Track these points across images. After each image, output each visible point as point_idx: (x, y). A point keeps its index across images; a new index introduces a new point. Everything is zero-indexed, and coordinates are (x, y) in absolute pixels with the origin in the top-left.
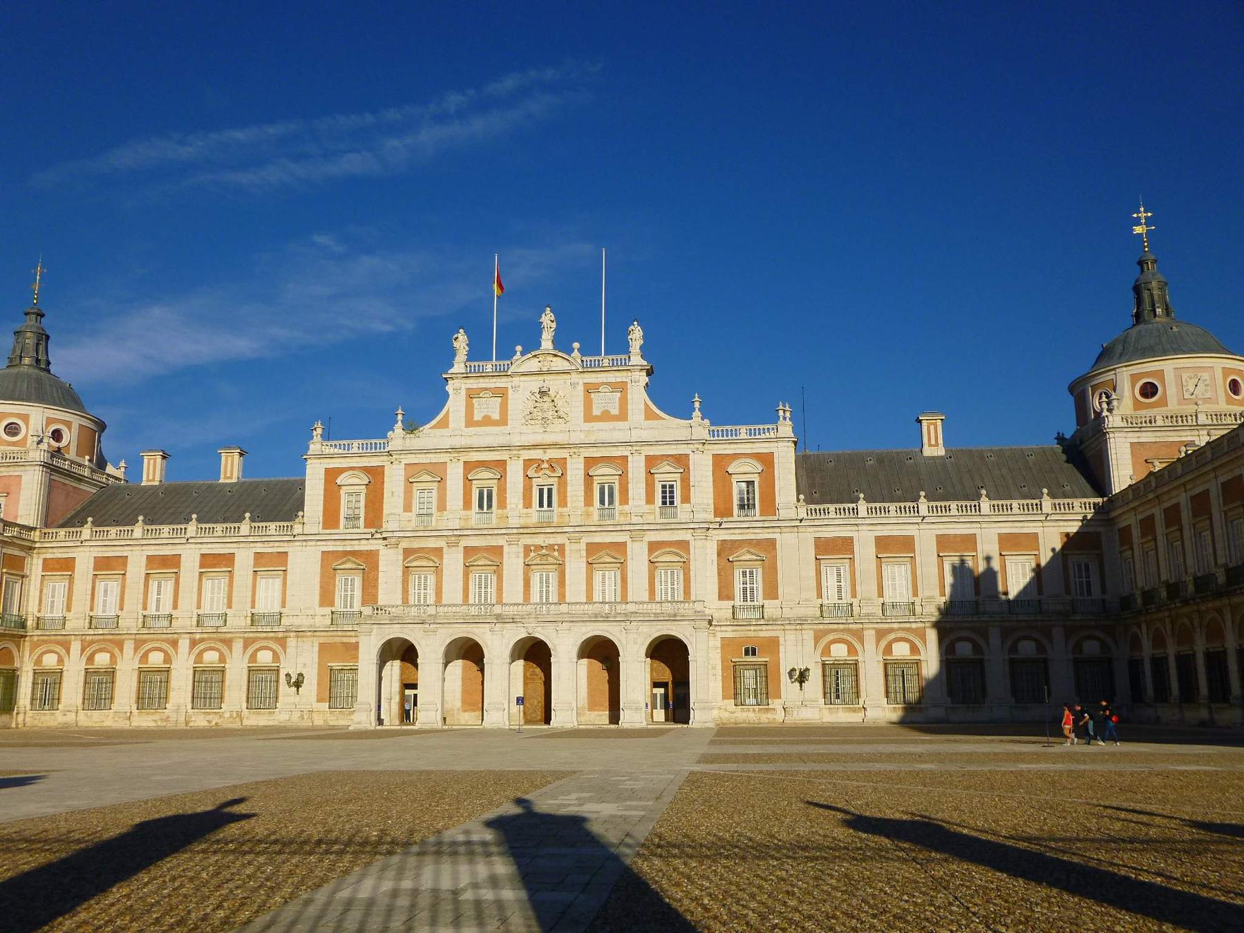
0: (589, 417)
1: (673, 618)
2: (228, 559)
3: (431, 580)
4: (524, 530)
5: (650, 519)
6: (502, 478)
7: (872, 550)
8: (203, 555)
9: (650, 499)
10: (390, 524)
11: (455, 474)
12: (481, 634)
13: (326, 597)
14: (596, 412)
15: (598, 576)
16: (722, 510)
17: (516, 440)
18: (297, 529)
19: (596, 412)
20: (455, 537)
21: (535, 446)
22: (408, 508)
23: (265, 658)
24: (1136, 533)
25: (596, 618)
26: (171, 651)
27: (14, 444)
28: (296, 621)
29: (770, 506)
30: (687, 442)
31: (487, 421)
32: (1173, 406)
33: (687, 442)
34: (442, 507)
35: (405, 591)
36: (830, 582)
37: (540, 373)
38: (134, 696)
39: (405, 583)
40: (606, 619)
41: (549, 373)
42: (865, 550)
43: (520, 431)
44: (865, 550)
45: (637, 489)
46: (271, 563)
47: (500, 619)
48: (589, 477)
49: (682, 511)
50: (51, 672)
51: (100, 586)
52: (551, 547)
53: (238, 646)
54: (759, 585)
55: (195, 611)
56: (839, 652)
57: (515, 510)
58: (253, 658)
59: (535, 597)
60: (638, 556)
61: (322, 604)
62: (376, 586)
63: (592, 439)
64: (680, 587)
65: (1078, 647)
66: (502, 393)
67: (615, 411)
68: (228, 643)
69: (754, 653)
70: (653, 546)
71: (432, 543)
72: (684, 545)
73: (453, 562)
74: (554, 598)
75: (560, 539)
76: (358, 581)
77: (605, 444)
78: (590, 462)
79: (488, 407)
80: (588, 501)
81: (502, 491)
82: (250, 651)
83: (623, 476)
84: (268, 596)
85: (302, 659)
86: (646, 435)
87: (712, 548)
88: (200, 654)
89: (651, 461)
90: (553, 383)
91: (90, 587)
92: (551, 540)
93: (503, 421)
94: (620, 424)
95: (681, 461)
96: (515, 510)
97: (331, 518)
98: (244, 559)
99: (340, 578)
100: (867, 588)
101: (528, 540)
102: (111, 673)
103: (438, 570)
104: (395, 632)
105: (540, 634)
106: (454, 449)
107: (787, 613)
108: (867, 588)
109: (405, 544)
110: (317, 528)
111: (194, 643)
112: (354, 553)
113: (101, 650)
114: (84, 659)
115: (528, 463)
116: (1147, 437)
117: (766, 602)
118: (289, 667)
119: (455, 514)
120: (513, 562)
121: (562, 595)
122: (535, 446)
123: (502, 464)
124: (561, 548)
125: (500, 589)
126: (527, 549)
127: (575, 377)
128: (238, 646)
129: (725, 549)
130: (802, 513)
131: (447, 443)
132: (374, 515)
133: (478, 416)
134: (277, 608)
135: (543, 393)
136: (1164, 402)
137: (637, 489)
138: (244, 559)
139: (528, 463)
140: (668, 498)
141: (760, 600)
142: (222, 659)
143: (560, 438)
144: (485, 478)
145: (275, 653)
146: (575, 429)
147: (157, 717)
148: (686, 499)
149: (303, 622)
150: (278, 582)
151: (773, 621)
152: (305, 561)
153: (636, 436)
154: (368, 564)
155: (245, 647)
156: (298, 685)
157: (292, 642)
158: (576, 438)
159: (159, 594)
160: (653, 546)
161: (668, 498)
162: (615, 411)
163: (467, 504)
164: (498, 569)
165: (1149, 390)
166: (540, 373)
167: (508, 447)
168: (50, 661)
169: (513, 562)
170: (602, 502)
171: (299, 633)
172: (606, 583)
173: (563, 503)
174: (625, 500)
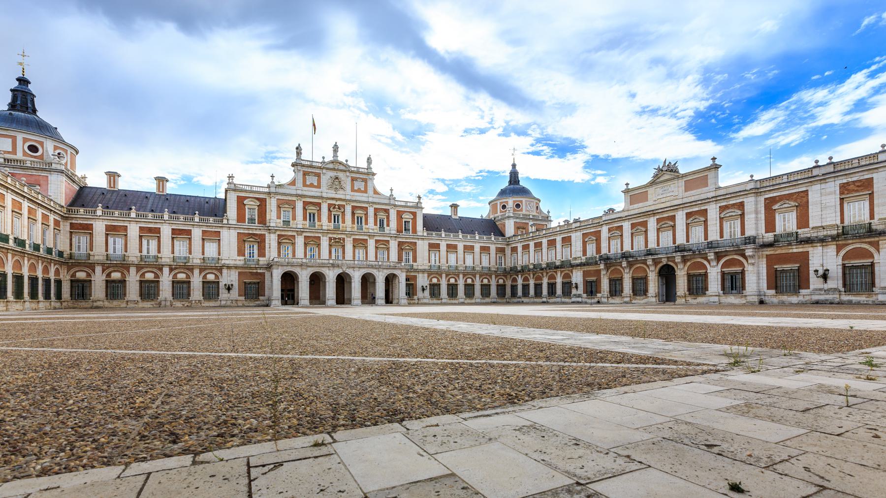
0: (353, 190)
3: (290, 248)
4: (328, 231)
7: (445, 248)
8: (173, 229)
9: (376, 224)
11: (299, 206)
13: (241, 252)
15: (357, 251)
16: (399, 231)
18: (225, 221)
19: (356, 188)
21: (333, 199)
22: (279, 217)
23: (211, 277)
24: (520, 249)
25: (369, 267)
26: (159, 273)
27: (35, 157)
28: (227, 262)
29: (415, 231)
30: (389, 204)
31: (312, 185)
32: (524, 212)
33: (389, 204)
34: (294, 218)
35: (279, 252)
36: (433, 258)
37: (334, 169)
38: (138, 293)
40: (372, 267)
41: (338, 170)
42: (443, 248)
44: (443, 248)
45: (371, 220)
46: (211, 236)
47: (333, 266)
48: (353, 214)
50: (83, 281)
51: (111, 240)
52: (339, 239)
53: (196, 272)
54: (411, 258)
55: (139, 254)
56: (435, 281)
57: (325, 222)
58: (205, 277)
59: (333, 257)
60: (371, 244)
61: (238, 255)
62: (264, 249)
65: (466, 281)
66: (318, 175)
70: (377, 241)
71: (290, 233)
73: (300, 241)
75: (343, 236)
76: (256, 247)
78: (354, 208)
79: (311, 180)
80: (353, 222)
82: (203, 274)
83: (366, 215)
84: (211, 250)
85: (230, 278)
88: (175, 275)
90: (341, 175)
91: (104, 239)
92: (340, 236)
93: (319, 186)
96: (325, 222)
97: (241, 218)
98: (197, 233)
99: (247, 245)
100: (443, 261)
101: (331, 236)
102: (123, 282)
103: (293, 244)
104: (289, 269)
106: (297, 195)
107: (420, 268)
108: (443, 261)
109: (278, 233)
110: (235, 222)
111: (171, 270)
113: (115, 271)
114: (104, 275)
115: (330, 205)
116: (518, 221)
117: (261, 259)
119: (300, 222)
120: (325, 243)
121: (344, 257)
123: (319, 205)
124: (344, 239)
125: (319, 254)
126: (330, 239)
127: (348, 174)
128: (196, 272)
129: (400, 244)
130: (425, 234)
132: (262, 219)
133: (308, 183)
134: (215, 255)
136: (522, 210)
137: (371, 220)
141: (411, 263)
142: (188, 276)
143: (342, 197)
144: (311, 209)
145: (216, 276)
146: (348, 194)
147: (153, 303)
148: (388, 225)
149: (231, 263)
152: (229, 238)
154: (261, 241)
155: (200, 273)
157: (225, 271)
158: (348, 197)
159: (148, 245)
160: (377, 241)
162: (363, 189)
163: (305, 219)
164: (319, 245)
165: (518, 206)
167: (322, 198)
168: (81, 275)
169: (325, 243)
171: (229, 267)
172: (360, 253)
173: (344, 222)
174: (366, 223)
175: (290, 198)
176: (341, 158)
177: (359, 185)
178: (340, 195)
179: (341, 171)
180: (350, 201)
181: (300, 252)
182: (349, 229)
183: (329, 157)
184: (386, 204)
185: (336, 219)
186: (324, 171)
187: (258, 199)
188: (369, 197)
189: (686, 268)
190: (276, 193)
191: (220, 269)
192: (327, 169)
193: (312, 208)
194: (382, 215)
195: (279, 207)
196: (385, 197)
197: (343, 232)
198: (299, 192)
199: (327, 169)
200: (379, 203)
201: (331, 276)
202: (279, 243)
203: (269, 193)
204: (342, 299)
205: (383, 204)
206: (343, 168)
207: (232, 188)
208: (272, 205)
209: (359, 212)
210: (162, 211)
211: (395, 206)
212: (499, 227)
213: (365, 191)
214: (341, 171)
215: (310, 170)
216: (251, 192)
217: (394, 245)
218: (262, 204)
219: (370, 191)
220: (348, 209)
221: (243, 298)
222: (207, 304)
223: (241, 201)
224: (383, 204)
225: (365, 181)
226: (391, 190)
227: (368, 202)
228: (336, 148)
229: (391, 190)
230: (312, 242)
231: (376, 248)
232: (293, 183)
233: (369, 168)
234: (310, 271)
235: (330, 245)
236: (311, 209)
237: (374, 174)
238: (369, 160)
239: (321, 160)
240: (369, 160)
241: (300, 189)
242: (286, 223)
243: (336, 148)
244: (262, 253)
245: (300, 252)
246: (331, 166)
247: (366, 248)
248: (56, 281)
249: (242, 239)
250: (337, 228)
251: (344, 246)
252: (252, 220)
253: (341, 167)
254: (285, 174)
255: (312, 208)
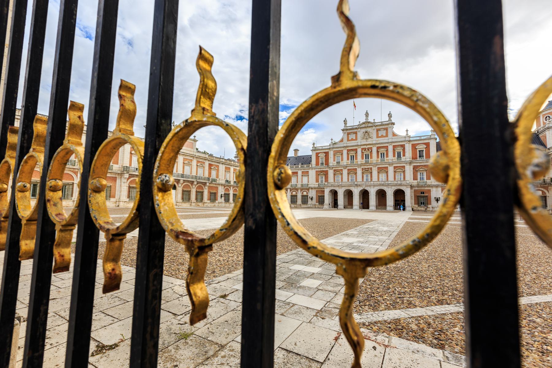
0: (378, 137)
1: (401, 185)
2: (297, 173)
3: (340, 176)
4: (362, 165)
5: (394, 161)
6: (356, 153)
9: (394, 156)
10: (331, 164)
11: (345, 152)
12: (352, 189)
13: (317, 181)
14: (380, 135)
16: (414, 158)
17: (359, 144)
18: (311, 166)
20: (345, 167)
21: (364, 145)
22: (334, 161)
23: (305, 193)
25: (380, 185)
34: (342, 160)
35: (334, 179)
37: (365, 127)
39: (334, 177)
40: (383, 185)
43: (360, 141)
46: (305, 174)
47: (357, 185)
48: (378, 152)
49: (403, 159)
53: (299, 191)
57: (360, 160)
58: (302, 193)
59: (365, 180)
60: (391, 170)
63: (379, 142)
64: (402, 177)
66: (356, 133)
67: (385, 135)
68: (297, 190)
69: (423, 193)
70: (395, 167)
71: (340, 168)
72: (404, 167)
73: (345, 172)
74: (369, 180)
75: (371, 167)
77: (382, 143)
78: (378, 148)
79: (353, 136)
80: (378, 157)
81: (356, 156)
83: (387, 151)
84: (305, 180)
85: (312, 193)
86: (394, 140)
87: (412, 167)
89: (394, 147)
90: (369, 130)
93: (356, 139)
94: (386, 138)
95: (403, 146)
96: (360, 160)
97: (317, 164)
98: (300, 173)
101: (363, 167)
103: (342, 174)
104: (333, 188)
105: (367, 188)
111: (291, 190)
112: (323, 171)
115: (362, 149)
118: (310, 195)
120: (359, 172)
121: (371, 180)
122: (364, 145)
123: (356, 150)
124: (371, 169)
126: (363, 169)
127: (374, 128)
128: (299, 191)
129: (415, 168)
131: (342, 146)
132: (327, 163)
133: (350, 139)
134: (307, 183)
135: (366, 132)
138: (300, 173)
139: (362, 149)
140: (399, 156)
142: (296, 193)
143: (370, 143)
144: (352, 153)
146: (374, 140)
148: (404, 155)
149: (312, 186)
150: (307, 178)
151: (429, 186)
152: (312, 173)
153: (390, 141)
154: (326, 174)
156: (312, 199)
157: (310, 190)
160: (395, 167)
161: (399, 156)
162: (385, 135)
163: (348, 159)
164: (356, 173)
166: (365, 127)
167: (358, 145)
169: (359, 172)
170: (381, 157)
171: (312, 188)
172: (383, 176)
173: (371, 158)
174: (387, 156)
175: (340, 149)
176: (371, 119)
177: (383, 133)
178: (370, 141)
179: (370, 127)
180: (375, 144)
181: (391, 177)
182: (374, 162)
183: (363, 120)
184: (402, 141)
185: (367, 157)
186: (359, 130)
187: (325, 153)
188: (390, 139)
189: (128, 182)
190: (333, 148)
191: (308, 189)
192: (361, 128)
193: (352, 152)
194: (400, 149)
195: (334, 155)
196: (402, 137)
197: (371, 164)
198: (345, 145)
199: (361, 128)
200: (396, 142)
201: (356, 192)
202: (334, 174)
203: (330, 149)
204: (349, 204)
205: (399, 142)
206: (371, 125)
207: (314, 149)
208: (331, 154)
209: (382, 151)
210: (299, 164)
211: (410, 141)
212: (542, 139)
213: (387, 136)
214: (370, 127)
215: (351, 131)
216: (322, 149)
217: (409, 170)
218: (327, 154)
219: (390, 135)
220: (374, 149)
221: (318, 204)
222: (303, 206)
223: (317, 154)
224: (399, 142)
225: (386, 129)
226: (407, 131)
227: (388, 143)
228: (367, 115)
229: (407, 131)
230: (352, 172)
231: (395, 172)
232: (342, 141)
233: (390, 120)
234: (344, 189)
235: (363, 173)
236: (352, 153)
237: (393, 124)
238: (390, 115)
239: (358, 123)
240: (390, 115)
241: (346, 143)
242: (338, 163)
243: (367, 115)
244: (327, 180)
245: (391, 177)
246: (363, 126)
247: (387, 172)
248: (234, 195)
249: (318, 174)
250: (367, 162)
251: (371, 173)
252: (322, 164)
253: (370, 125)
254: (338, 136)
255: (352, 152)
